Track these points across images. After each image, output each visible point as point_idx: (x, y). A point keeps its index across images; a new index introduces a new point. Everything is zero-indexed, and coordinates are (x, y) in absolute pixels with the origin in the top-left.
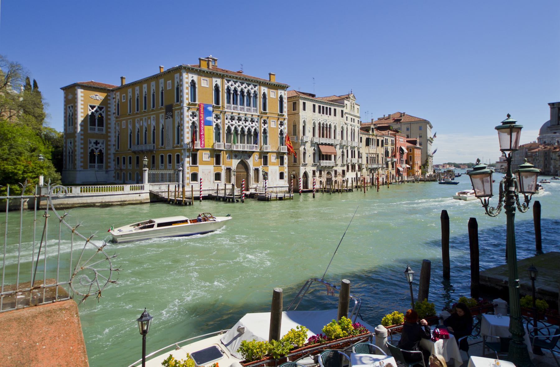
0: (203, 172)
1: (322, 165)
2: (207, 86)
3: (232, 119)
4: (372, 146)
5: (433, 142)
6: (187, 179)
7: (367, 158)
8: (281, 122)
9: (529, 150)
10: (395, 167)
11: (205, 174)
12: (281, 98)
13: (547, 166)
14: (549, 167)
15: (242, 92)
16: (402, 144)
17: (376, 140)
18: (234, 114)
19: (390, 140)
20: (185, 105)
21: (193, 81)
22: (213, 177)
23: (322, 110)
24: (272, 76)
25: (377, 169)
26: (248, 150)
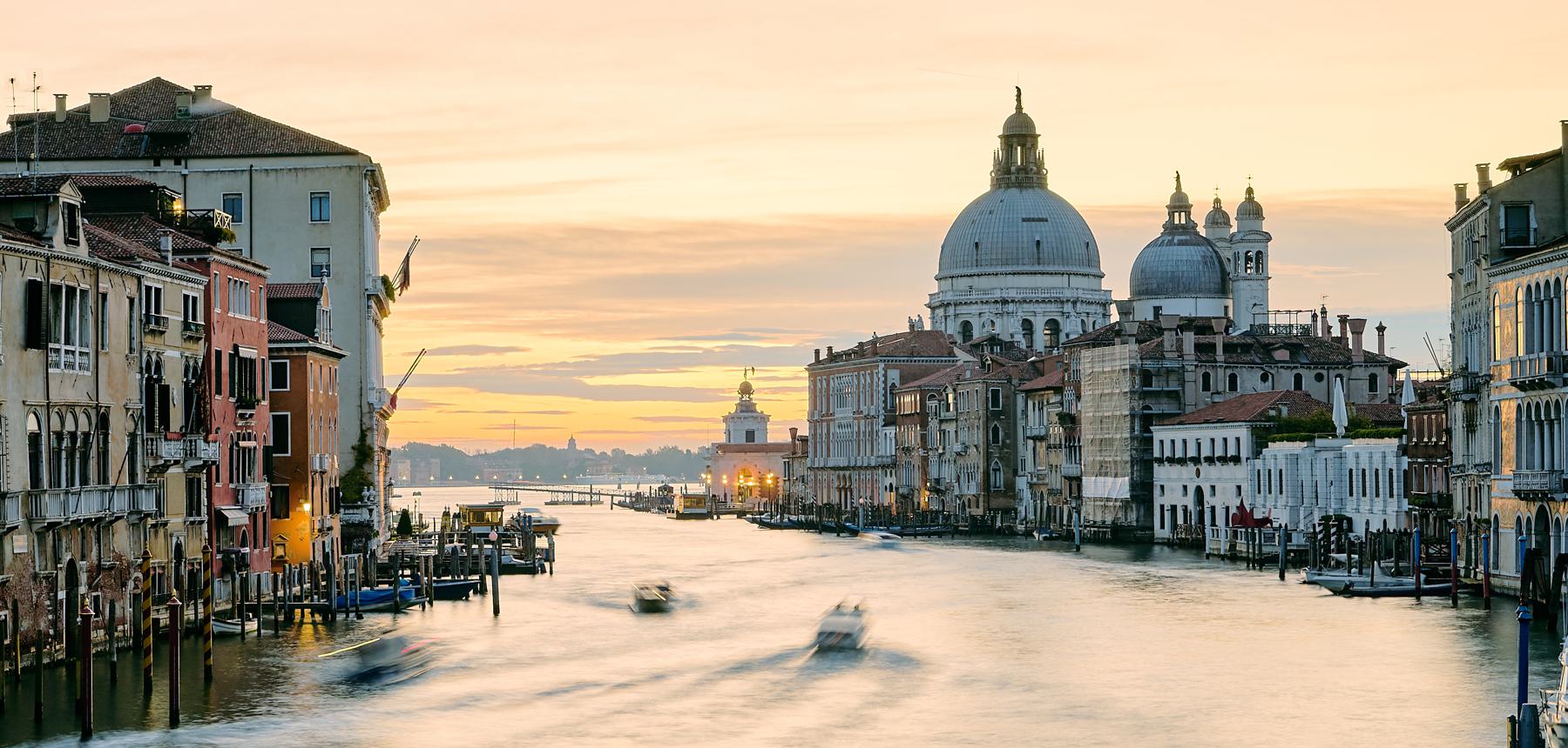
4: (64, 348)
5: (392, 306)
7: (34, 439)
9: (903, 380)
10: (204, 510)
14: (1010, 487)
16: (242, 328)
17: (91, 301)
19: (176, 290)
25: (101, 526)
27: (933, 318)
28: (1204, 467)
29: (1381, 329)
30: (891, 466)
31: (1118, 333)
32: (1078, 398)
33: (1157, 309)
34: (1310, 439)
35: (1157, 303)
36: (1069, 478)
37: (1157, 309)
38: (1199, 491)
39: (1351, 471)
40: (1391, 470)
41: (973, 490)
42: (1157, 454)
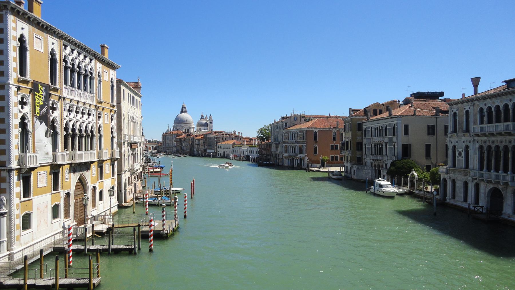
0: (38, 209)
1: (135, 169)
2: (42, 51)
3: (70, 111)
6: (17, 229)
8: (112, 116)
11: (41, 212)
12: (112, 82)
13: (192, 149)
14: (193, 150)
15: (79, 67)
18: (73, 103)
20: (11, 81)
21: (22, 36)
22: (50, 215)
23: (132, 101)
24: (105, 49)
26: (90, 160)
27: (173, 128)
28: (225, 149)
29: (241, 133)
30: (175, 147)
31: (211, 133)
32: (206, 140)
33: (200, 128)
34: (241, 146)
35: (200, 127)
36: (204, 150)
37: (200, 128)
38: (224, 152)
39: (249, 151)
40: (256, 151)
41: (189, 151)
42: (218, 147)
